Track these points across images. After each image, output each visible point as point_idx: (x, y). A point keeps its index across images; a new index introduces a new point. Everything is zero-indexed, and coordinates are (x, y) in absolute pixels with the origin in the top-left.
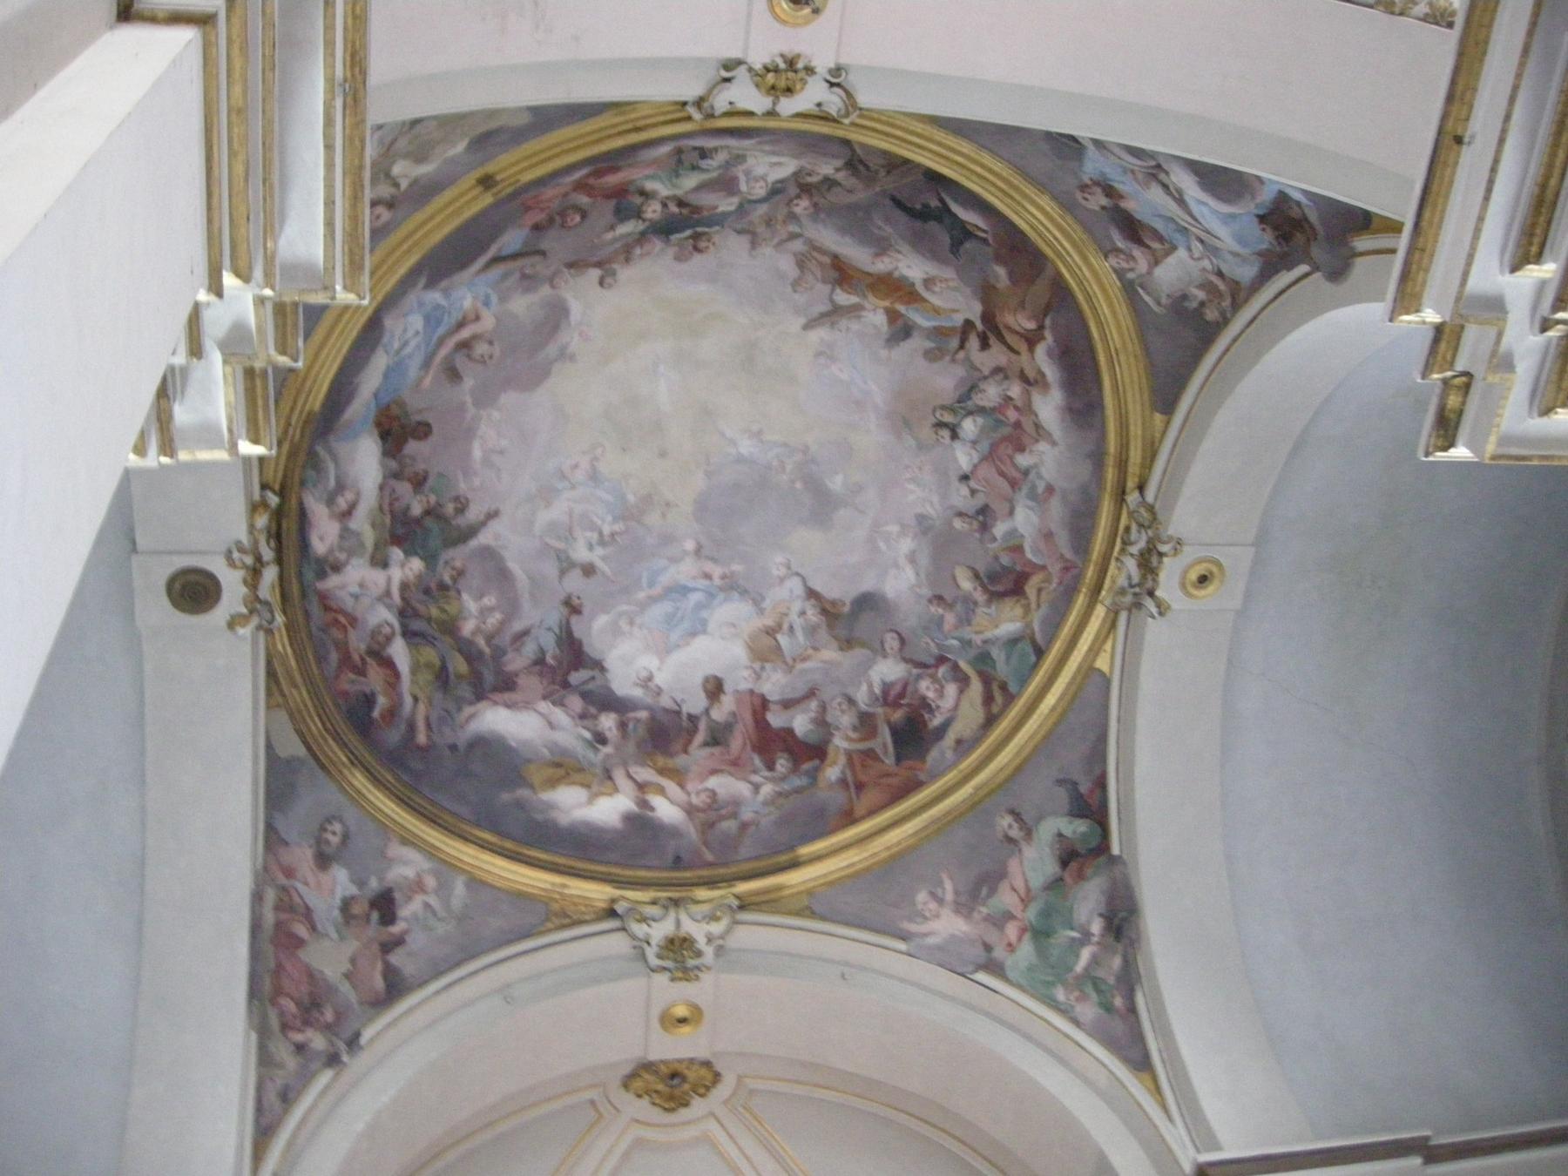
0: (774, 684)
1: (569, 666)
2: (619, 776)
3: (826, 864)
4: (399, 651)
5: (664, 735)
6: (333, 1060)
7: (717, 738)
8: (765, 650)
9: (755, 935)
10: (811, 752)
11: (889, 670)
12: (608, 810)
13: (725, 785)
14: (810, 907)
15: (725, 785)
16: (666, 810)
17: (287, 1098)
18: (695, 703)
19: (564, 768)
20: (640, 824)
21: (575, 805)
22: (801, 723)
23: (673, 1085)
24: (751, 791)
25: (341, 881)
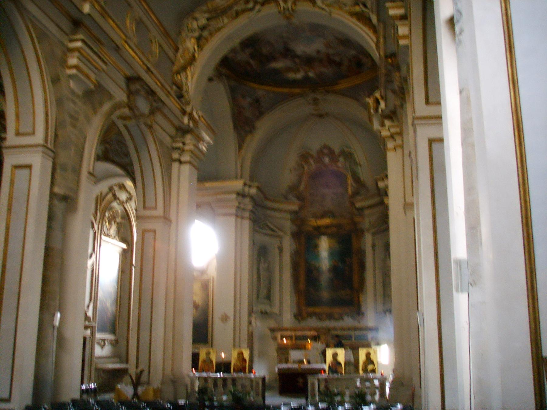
0: (331, 51)
1: (287, 53)
2: (301, 70)
3: (343, 85)
4: (252, 62)
5: (309, 61)
6: (251, 132)
7: (321, 61)
8: (328, 46)
9: (331, 97)
10: (339, 64)
11: (353, 52)
12: (299, 76)
13: (323, 70)
14: (342, 93)
15: (323, 70)
16: (311, 74)
17: (243, 141)
18: (314, 54)
19: (289, 70)
20: (306, 78)
21: (292, 76)
22: (337, 59)
23: (321, 116)
24: (328, 71)
25: (249, 100)
